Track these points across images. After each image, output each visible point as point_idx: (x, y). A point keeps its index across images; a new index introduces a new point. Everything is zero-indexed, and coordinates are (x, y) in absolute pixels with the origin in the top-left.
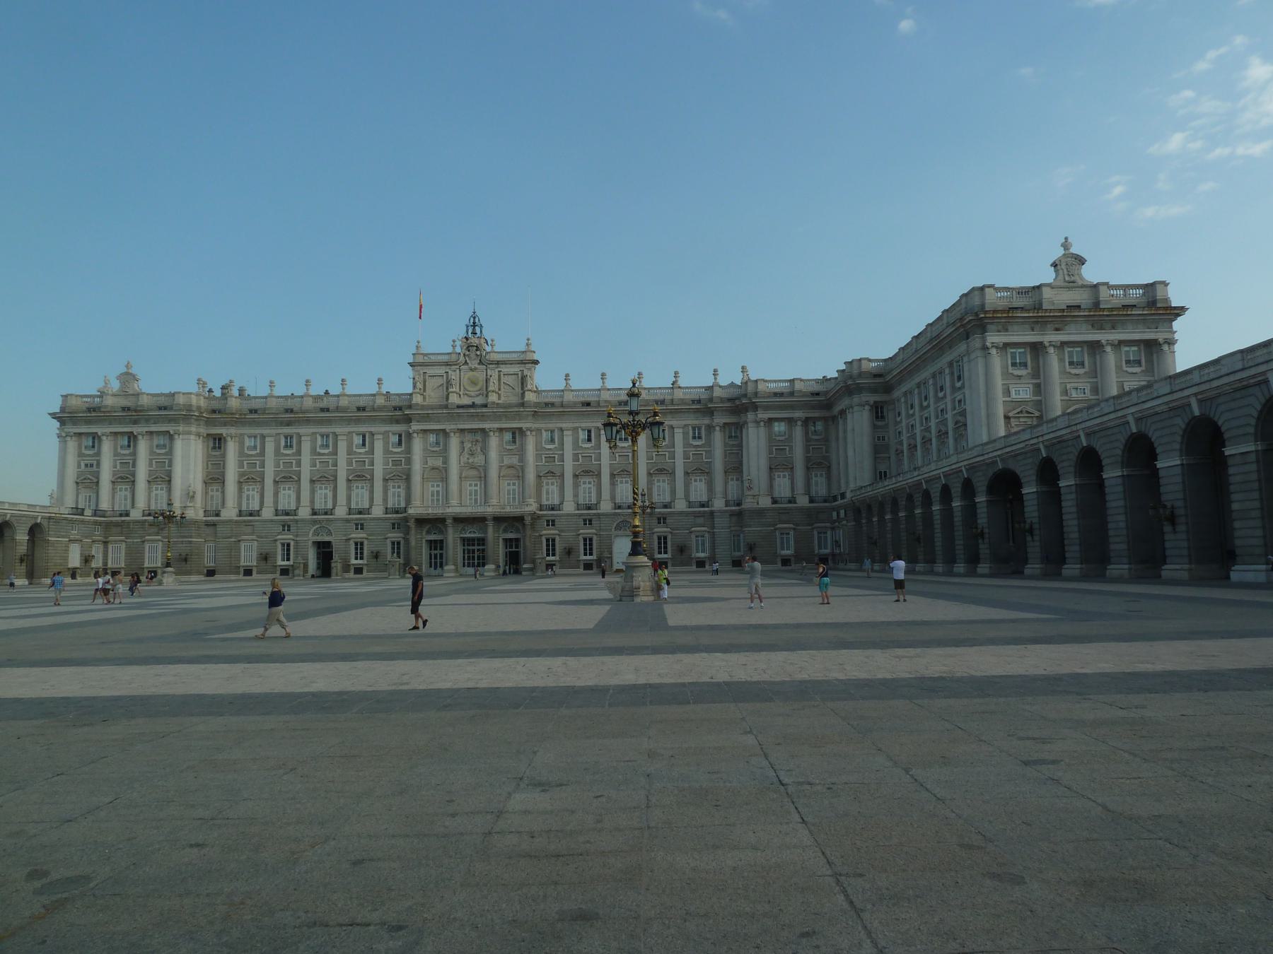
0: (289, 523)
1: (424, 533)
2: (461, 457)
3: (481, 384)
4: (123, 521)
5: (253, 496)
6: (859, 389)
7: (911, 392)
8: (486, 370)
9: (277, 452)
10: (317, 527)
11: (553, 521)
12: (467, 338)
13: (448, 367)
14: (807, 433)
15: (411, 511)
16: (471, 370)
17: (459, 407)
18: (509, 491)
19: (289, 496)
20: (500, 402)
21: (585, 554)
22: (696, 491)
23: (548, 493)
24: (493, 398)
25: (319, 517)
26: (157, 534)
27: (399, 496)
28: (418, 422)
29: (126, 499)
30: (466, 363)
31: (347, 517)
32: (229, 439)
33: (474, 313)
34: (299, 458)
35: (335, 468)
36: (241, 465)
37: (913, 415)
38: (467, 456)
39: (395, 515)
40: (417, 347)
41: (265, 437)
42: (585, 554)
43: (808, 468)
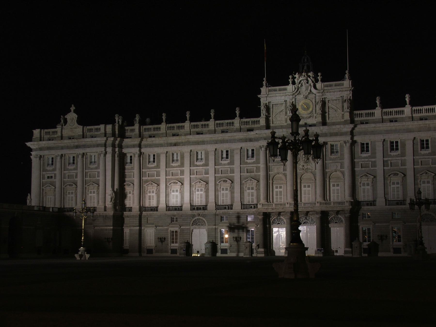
5: (153, 196)
8: (315, 97)
18: (334, 190)
19: (177, 196)
23: (364, 192)
27: (252, 196)
29: (72, 200)
35: (207, 176)
38: (302, 164)
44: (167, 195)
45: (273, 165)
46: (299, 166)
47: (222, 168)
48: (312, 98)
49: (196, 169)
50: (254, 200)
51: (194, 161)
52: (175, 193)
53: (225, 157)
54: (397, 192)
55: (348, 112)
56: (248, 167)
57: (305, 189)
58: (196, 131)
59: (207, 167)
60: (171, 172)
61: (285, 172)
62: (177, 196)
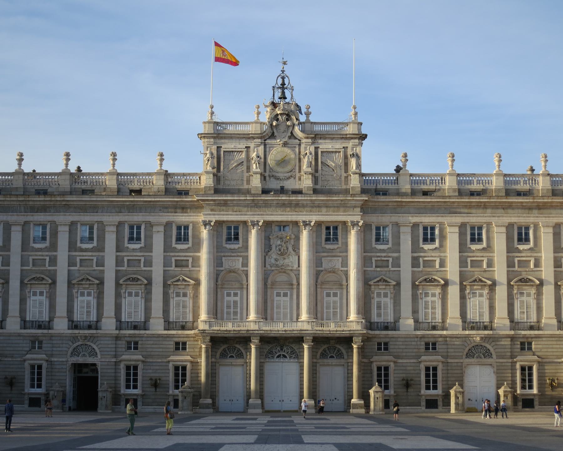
0: (41, 338)
1: (218, 355)
2: (267, 257)
3: (293, 162)
8: (300, 145)
9: (25, 246)
10: (77, 344)
11: (386, 344)
12: (274, 105)
13: (249, 141)
15: (202, 326)
20: (318, 187)
21: (428, 388)
23: (379, 307)
25: (81, 332)
28: (212, 210)
31: (117, 332)
33: (283, 71)
34: (55, 253)
39: (180, 332)
40: (212, 113)
41: (10, 225)
42: (428, 388)
44: (23, 301)
45: (224, 256)
47: (128, 256)
48: (295, 146)
49: (80, 256)
50: (188, 315)
51: (77, 241)
52: (38, 298)
53: (88, 236)
54: (432, 308)
55: (356, 173)
56: (178, 256)
57: (278, 298)
58: (81, 188)
59: (101, 254)
60: (31, 259)
61: (245, 269)
62: (41, 303)
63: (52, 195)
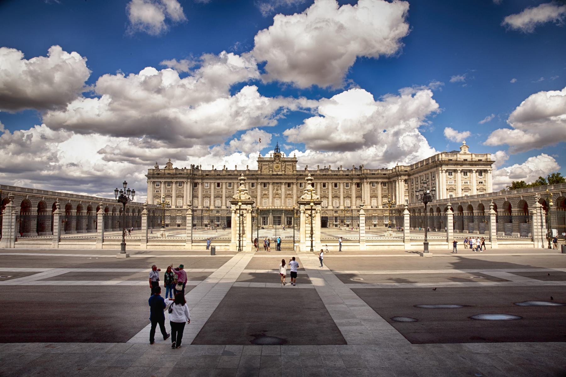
4: (169, 209)
5: (207, 202)
6: (400, 175)
7: (417, 178)
14: (382, 186)
16: (278, 163)
17: (273, 175)
19: (219, 202)
22: (347, 203)
24: (283, 173)
26: (180, 213)
28: (260, 179)
30: (275, 161)
32: (200, 184)
36: (203, 191)
37: (418, 184)
43: (382, 197)
46: (275, 191)
52: (218, 201)
63: (221, 176)
